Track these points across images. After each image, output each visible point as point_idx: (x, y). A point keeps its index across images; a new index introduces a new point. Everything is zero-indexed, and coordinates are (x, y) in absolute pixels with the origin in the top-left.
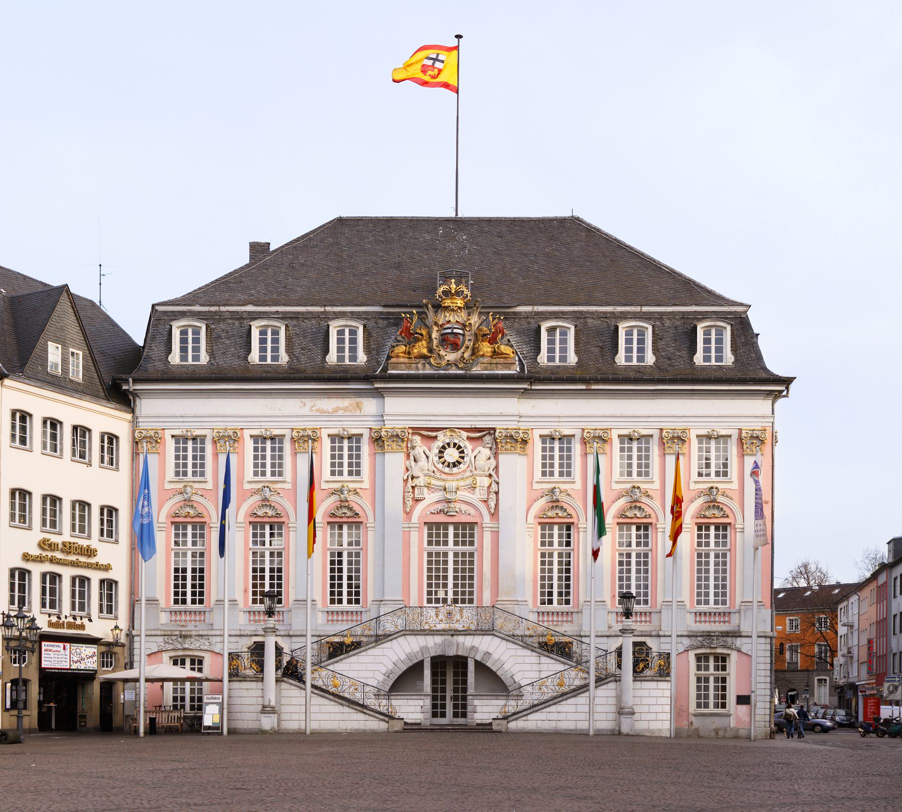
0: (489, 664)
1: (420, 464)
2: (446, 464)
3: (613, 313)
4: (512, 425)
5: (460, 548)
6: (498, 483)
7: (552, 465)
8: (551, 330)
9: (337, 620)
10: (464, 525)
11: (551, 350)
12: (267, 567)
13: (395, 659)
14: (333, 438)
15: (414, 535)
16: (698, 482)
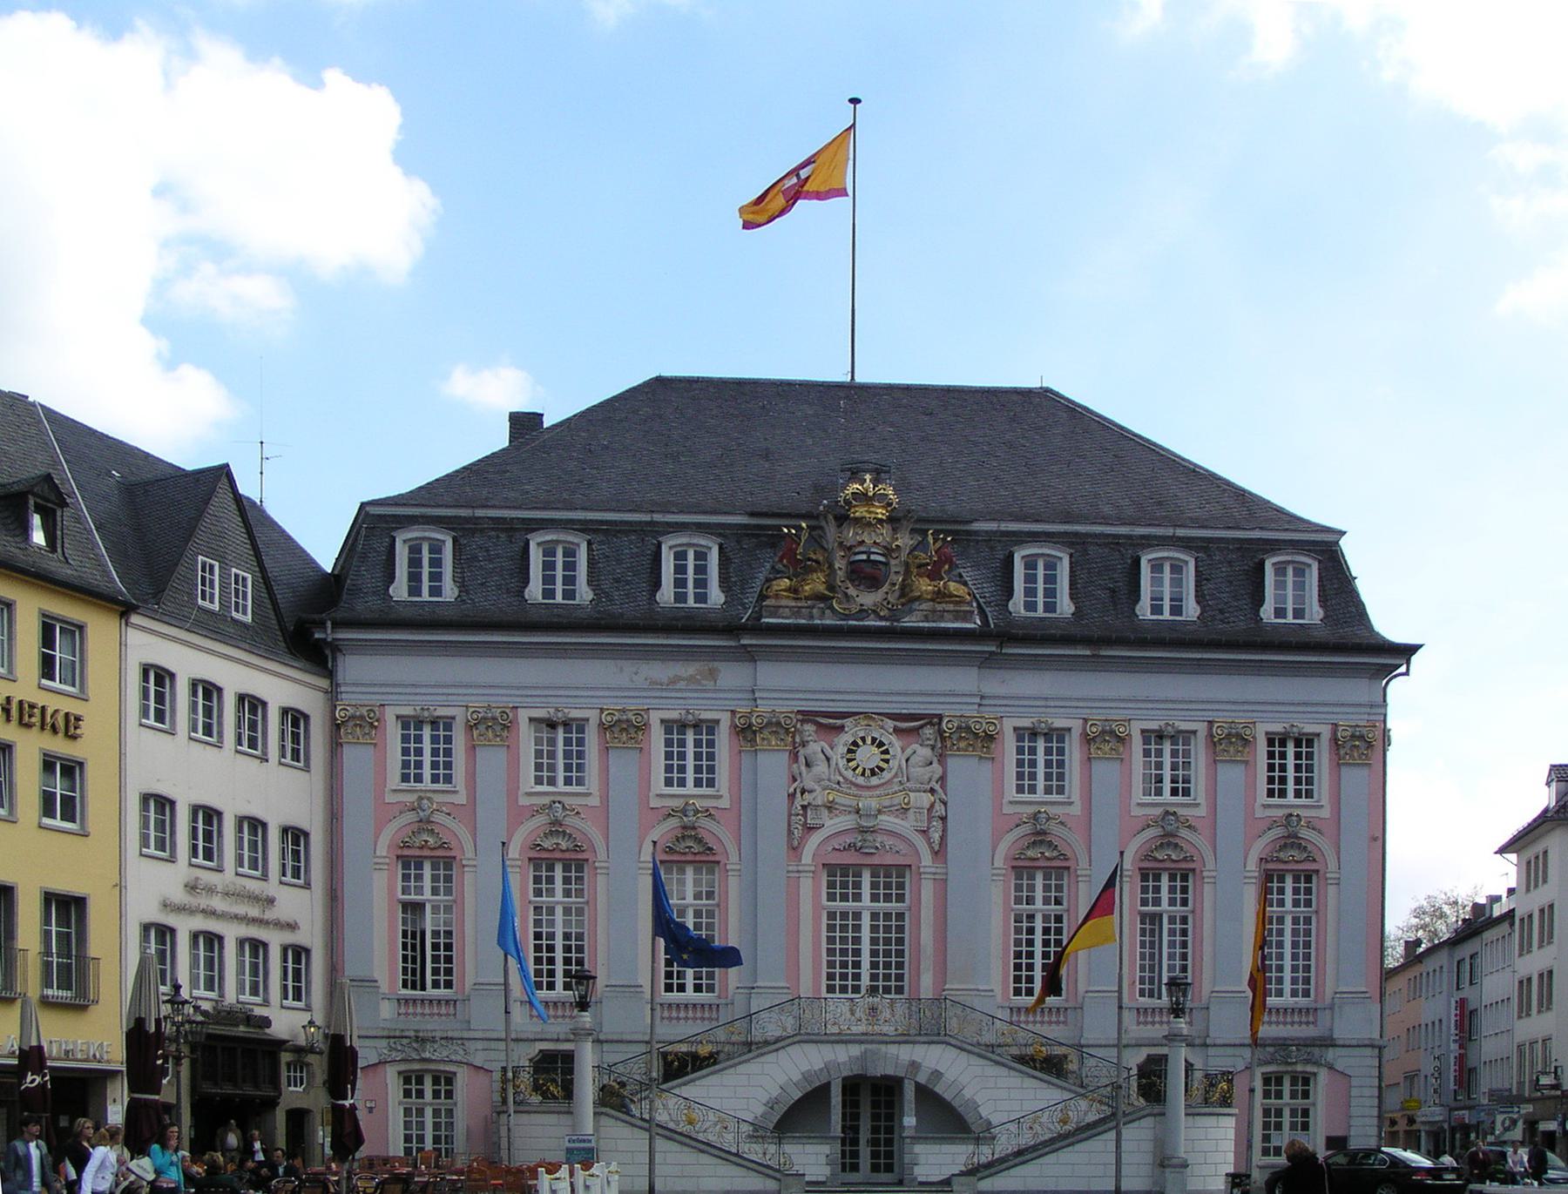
0: (938, 1089)
1: (816, 770)
2: (859, 770)
3: (1129, 537)
4: (970, 711)
5: (882, 906)
6: (945, 804)
7: (1033, 776)
8: (1030, 564)
9: (678, 1019)
10: (888, 869)
11: (1030, 592)
12: (559, 932)
13: (782, 1079)
14: (668, 725)
15: (806, 885)
16: (1269, 806)
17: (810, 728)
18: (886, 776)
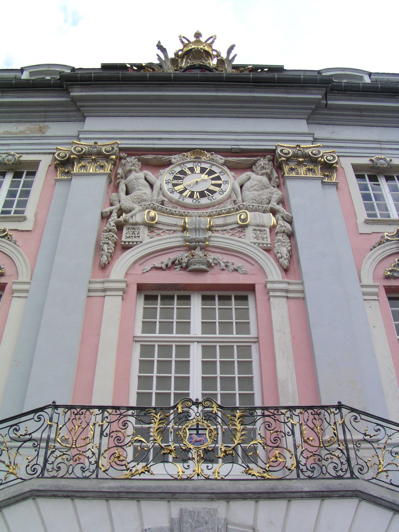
2: (187, 193)
15: (113, 306)
17: (132, 160)
18: (218, 197)
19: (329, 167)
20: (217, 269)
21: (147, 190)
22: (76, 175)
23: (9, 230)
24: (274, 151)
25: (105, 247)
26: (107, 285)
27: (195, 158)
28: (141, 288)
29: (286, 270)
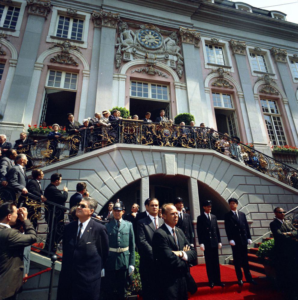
17: (125, 23)
19: (198, 40)
20: (157, 75)
21: (131, 38)
22: (103, 26)
23: (78, 47)
24: (179, 30)
25: (118, 61)
26: (120, 76)
27: (149, 28)
28: (131, 78)
29: (180, 78)
